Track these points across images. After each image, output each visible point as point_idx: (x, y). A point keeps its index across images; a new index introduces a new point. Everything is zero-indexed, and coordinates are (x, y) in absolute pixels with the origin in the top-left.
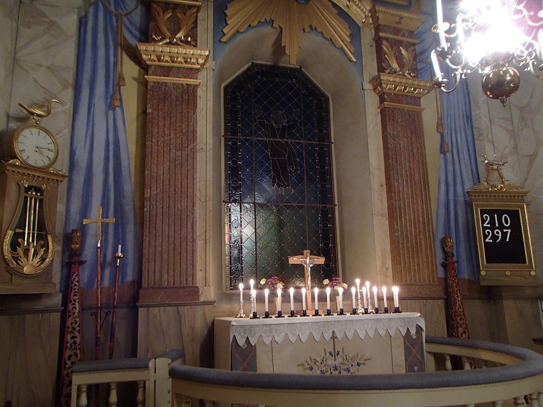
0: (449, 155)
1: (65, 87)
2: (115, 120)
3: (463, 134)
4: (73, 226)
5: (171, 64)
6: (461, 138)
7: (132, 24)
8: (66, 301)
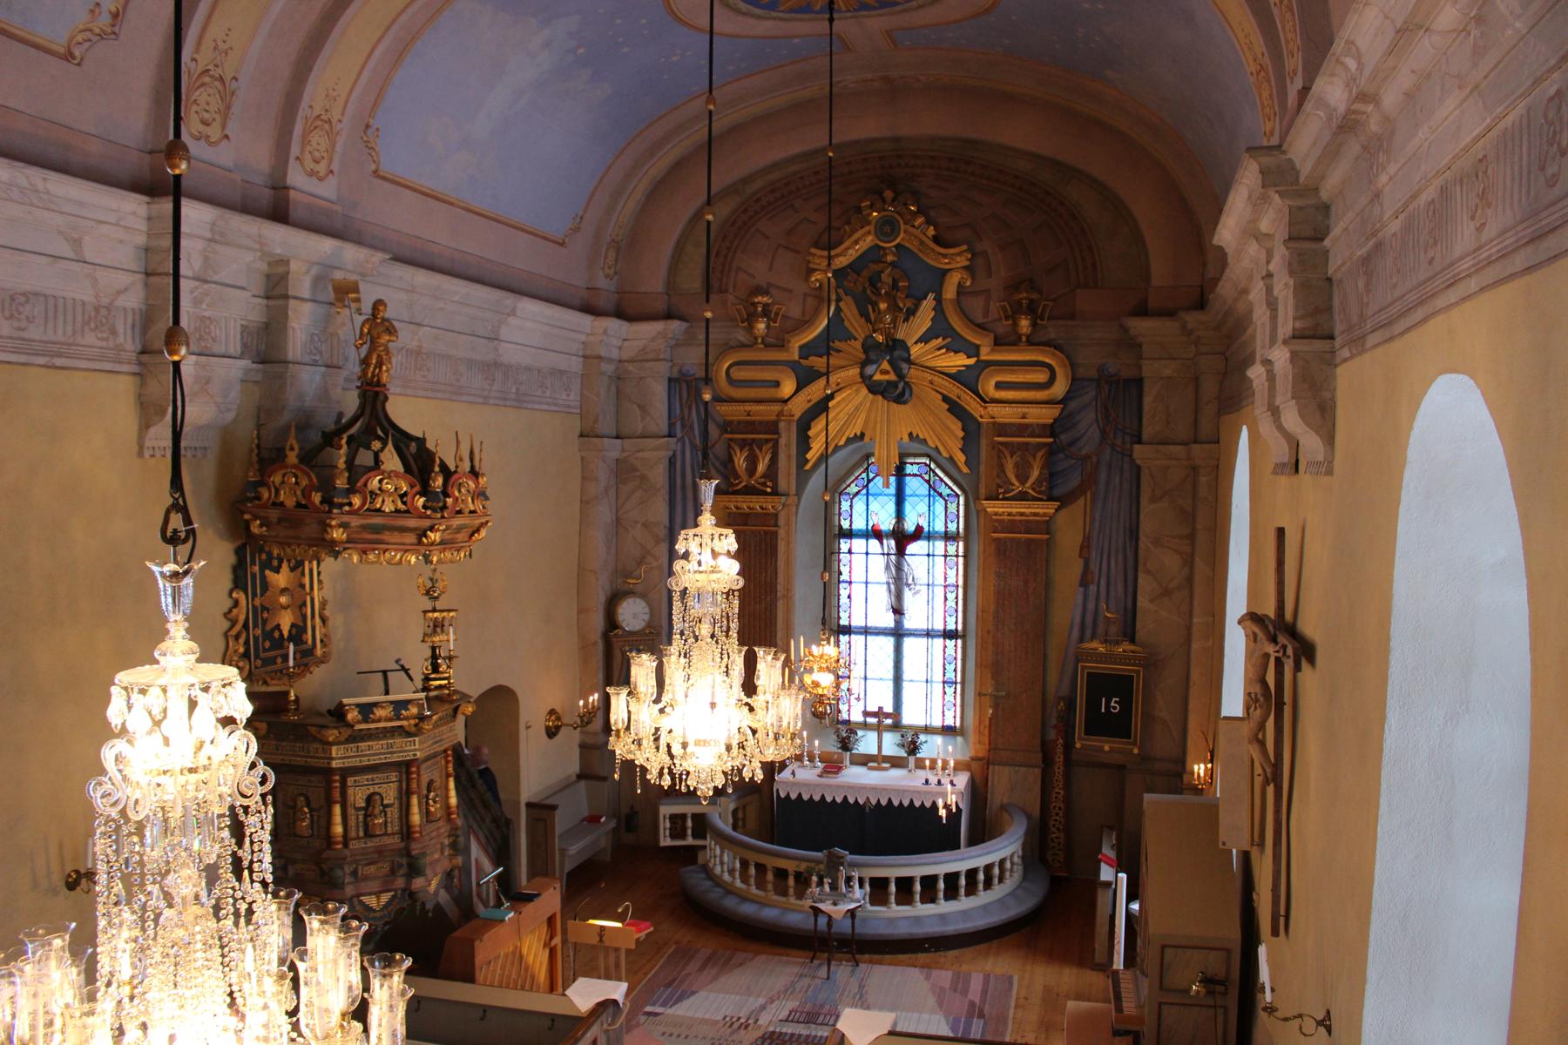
0: (1093, 588)
1: (657, 543)
3: (1120, 556)
7: (717, 458)
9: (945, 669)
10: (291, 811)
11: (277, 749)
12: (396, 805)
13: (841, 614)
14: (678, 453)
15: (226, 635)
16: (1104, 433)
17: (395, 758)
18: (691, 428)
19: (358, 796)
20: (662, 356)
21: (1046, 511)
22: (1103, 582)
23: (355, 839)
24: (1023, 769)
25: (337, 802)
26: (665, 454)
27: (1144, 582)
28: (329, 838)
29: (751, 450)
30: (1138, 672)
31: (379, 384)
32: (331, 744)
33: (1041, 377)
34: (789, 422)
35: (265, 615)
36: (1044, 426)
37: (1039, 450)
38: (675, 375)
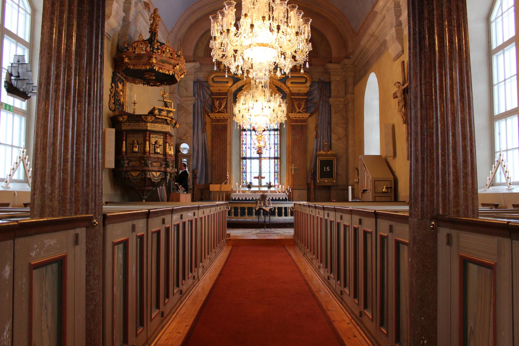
0: (319, 139)
1: (190, 129)
2: (204, 136)
4: (194, 168)
5: (219, 118)
6: (325, 132)
7: (208, 104)
8: (193, 187)
9: (275, 168)
10: (131, 145)
11: (129, 125)
12: (162, 146)
13: (244, 153)
14: (196, 103)
15: (110, 96)
16: (320, 96)
17: (164, 130)
18: (200, 96)
19: (153, 141)
20: (192, 74)
21: (306, 116)
22: (322, 137)
23: (151, 154)
24: (302, 191)
25: (147, 141)
26: (193, 102)
27: (334, 136)
28: (145, 152)
29: (220, 101)
30: (334, 159)
31: (156, 30)
32: (147, 122)
33: (303, 80)
34: (231, 93)
35: (118, 94)
36: (305, 93)
37: (304, 100)
38: (196, 80)
